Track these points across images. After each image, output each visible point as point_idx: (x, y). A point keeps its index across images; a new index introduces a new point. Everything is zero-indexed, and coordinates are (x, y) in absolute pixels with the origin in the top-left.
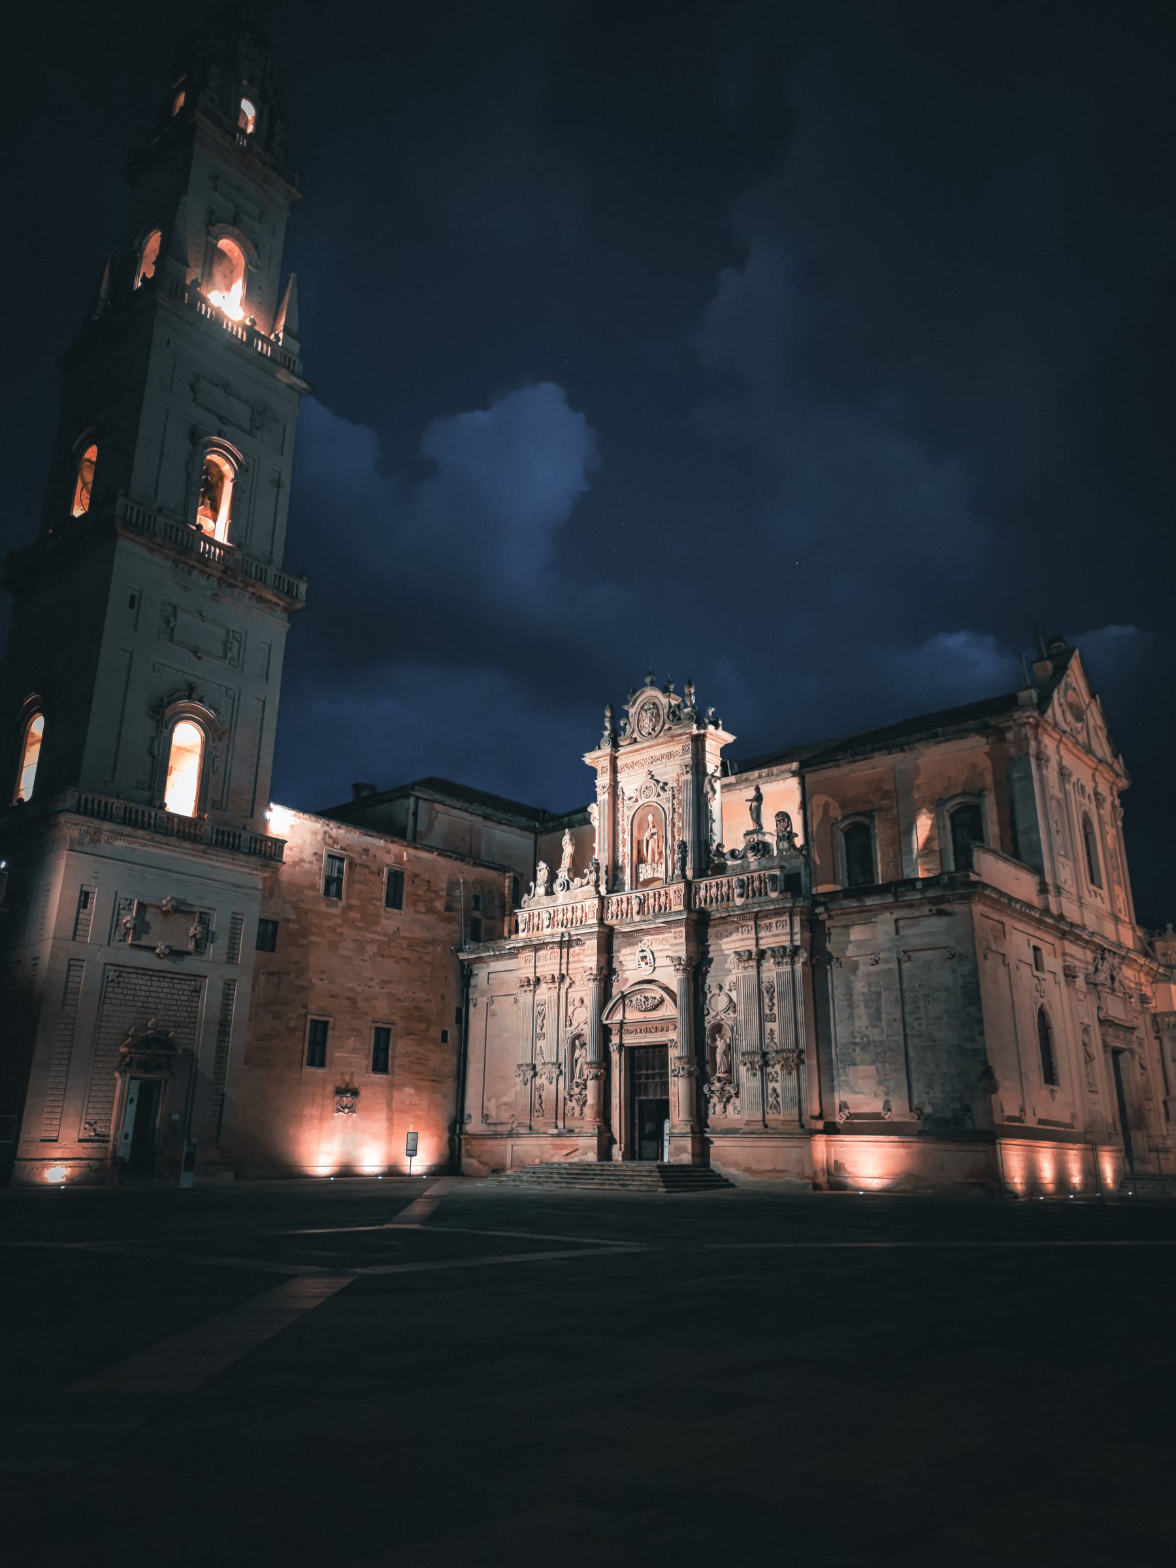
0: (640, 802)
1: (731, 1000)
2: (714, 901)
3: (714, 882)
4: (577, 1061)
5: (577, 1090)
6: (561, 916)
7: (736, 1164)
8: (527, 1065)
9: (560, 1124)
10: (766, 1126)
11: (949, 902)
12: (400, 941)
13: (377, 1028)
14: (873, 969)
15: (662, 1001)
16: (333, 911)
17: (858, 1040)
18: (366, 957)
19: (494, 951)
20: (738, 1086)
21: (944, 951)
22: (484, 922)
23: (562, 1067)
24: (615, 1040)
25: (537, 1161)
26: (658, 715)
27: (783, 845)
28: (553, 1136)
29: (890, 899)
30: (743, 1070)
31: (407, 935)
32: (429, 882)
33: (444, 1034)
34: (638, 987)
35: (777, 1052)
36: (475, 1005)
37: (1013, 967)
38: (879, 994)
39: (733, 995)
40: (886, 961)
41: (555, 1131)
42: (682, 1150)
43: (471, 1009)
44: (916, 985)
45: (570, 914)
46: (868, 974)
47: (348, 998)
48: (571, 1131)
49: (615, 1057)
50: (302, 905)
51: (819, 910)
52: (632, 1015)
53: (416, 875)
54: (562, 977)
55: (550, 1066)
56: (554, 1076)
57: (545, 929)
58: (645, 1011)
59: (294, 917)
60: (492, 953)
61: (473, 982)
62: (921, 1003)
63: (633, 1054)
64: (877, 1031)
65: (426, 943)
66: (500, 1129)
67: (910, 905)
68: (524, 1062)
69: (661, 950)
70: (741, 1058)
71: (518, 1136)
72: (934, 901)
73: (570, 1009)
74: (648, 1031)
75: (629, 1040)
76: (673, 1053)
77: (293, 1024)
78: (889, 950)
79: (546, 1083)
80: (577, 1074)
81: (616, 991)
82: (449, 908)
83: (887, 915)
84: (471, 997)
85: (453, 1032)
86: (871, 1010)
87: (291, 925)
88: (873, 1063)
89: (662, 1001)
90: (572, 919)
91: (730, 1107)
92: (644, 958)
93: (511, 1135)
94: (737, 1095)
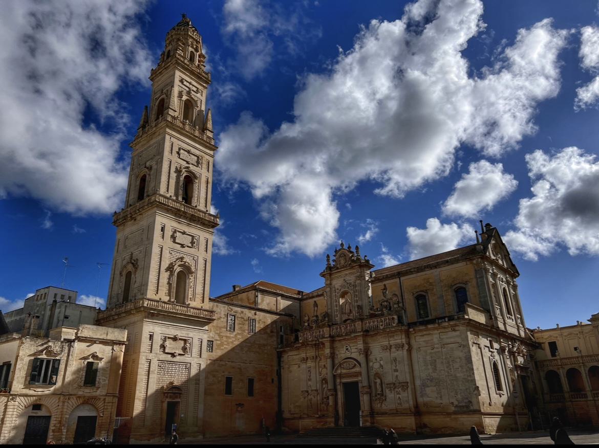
0: (342, 291)
1: (381, 365)
3: (372, 321)
5: (325, 400)
6: (315, 334)
8: (306, 391)
9: (319, 413)
10: (397, 411)
11: (458, 326)
12: (255, 345)
13: (249, 379)
14: (432, 351)
15: (355, 365)
16: (232, 335)
17: (429, 378)
18: (244, 352)
20: (386, 396)
21: (457, 344)
22: (284, 336)
24: (338, 381)
25: (311, 428)
26: (346, 259)
28: (317, 418)
29: (437, 325)
30: (387, 391)
31: (258, 343)
32: (264, 322)
33: (273, 380)
34: (344, 361)
35: (399, 383)
36: (283, 369)
37: (482, 349)
38: (435, 361)
39: (382, 362)
40: (437, 348)
41: (318, 416)
42: (367, 421)
43: (282, 370)
44: (448, 356)
45: (318, 333)
46: (431, 353)
47: (238, 368)
48: (324, 415)
49: (339, 387)
50: (221, 334)
51: (411, 330)
52: (344, 371)
53: (260, 320)
54: (316, 357)
56: (316, 395)
59: (219, 339)
61: (282, 360)
62: (451, 363)
63: (346, 385)
64: (436, 374)
65: (264, 345)
66: (295, 415)
67: (444, 328)
68: (303, 390)
69: (354, 346)
70: (386, 386)
71: (304, 418)
72: (452, 326)
73: (320, 369)
74: (351, 376)
75: (344, 380)
76: (360, 385)
77: (220, 379)
78: (438, 344)
79: (313, 397)
80: (324, 394)
81: (336, 362)
82: (272, 332)
83: (436, 332)
84: (282, 365)
85: (276, 379)
86: (433, 367)
87: (218, 342)
88: (435, 386)
89: (355, 365)
91: (383, 405)
92: (347, 349)
93: (301, 418)
94: (386, 399)
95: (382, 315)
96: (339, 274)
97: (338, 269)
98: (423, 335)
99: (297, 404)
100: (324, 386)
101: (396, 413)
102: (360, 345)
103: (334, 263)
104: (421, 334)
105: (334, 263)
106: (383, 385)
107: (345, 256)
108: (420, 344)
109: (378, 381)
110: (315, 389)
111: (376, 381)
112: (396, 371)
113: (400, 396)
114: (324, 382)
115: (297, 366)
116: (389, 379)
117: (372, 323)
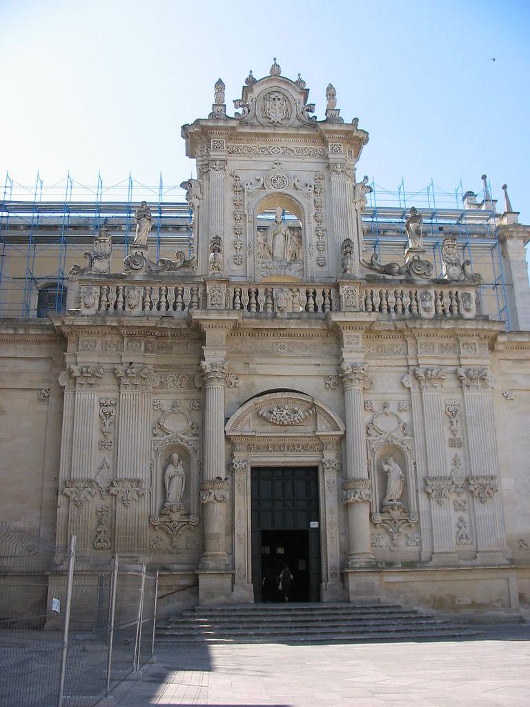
2: (392, 310)
4: (171, 479)
7: (423, 601)
19: (15, 329)
23: (146, 486)
24: (239, 456)
27: (454, 270)
39: (405, 417)
45: (171, 296)
55: (127, 484)
57: (127, 309)
58: (288, 425)
60: (11, 332)
63: (258, 473)
69: (310, 357)
74: (291, 448)
79: (119, 505)
90: (176, 302)
95: (409, 282)
96: (262, 143)
97: (252, 126)
98: (521, 361)
99: (20, 525)
100: (171, 470)
101: (469, 564)
102: (353, 355)
103: (240, 110)
104: (516, 357)
105: (240, 110)
106: (412, 482)
107: (286, 99)
108: (515, 382)
109: (394, 469)
110: (131, 476)
111: (386, 468)
112: (454, 443)
113: (466, 516)
114: (175, 456)
115: (34, 395)
116: (442, 461)
117: (392, 299)
